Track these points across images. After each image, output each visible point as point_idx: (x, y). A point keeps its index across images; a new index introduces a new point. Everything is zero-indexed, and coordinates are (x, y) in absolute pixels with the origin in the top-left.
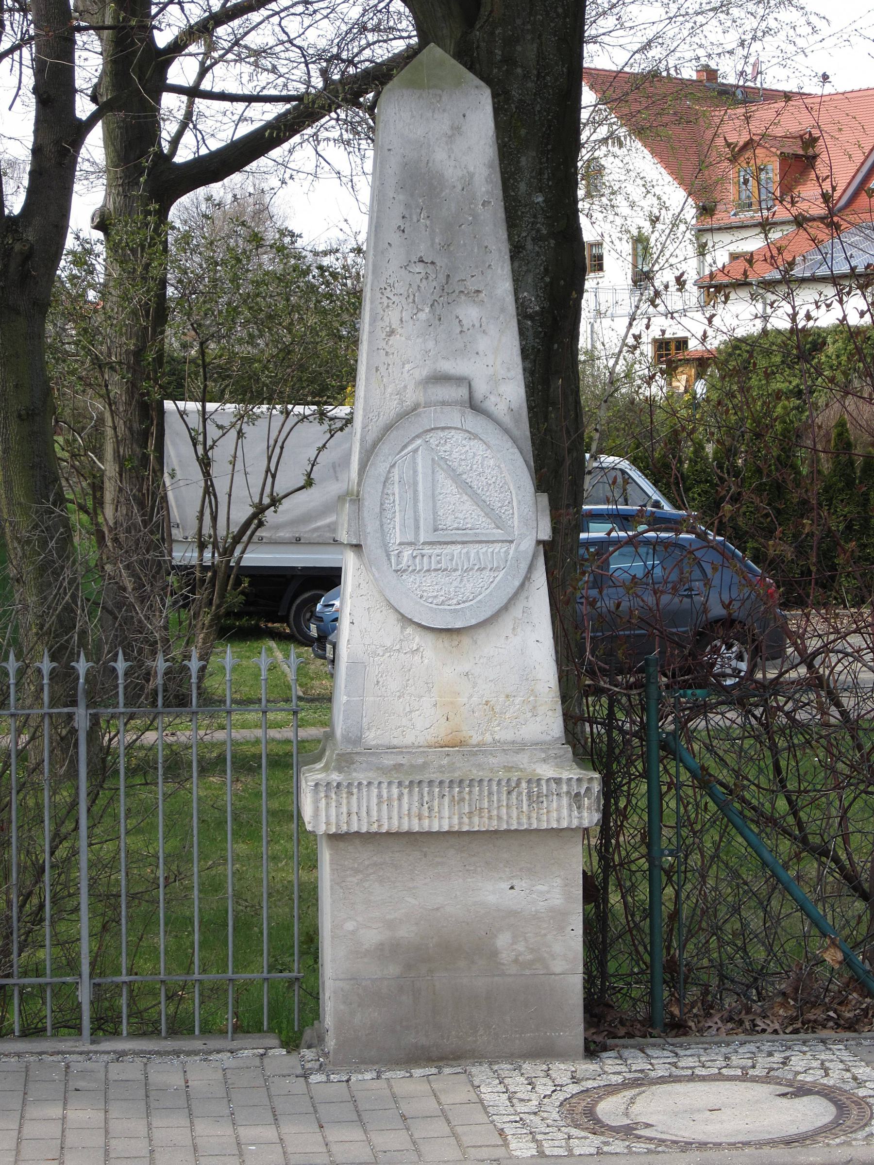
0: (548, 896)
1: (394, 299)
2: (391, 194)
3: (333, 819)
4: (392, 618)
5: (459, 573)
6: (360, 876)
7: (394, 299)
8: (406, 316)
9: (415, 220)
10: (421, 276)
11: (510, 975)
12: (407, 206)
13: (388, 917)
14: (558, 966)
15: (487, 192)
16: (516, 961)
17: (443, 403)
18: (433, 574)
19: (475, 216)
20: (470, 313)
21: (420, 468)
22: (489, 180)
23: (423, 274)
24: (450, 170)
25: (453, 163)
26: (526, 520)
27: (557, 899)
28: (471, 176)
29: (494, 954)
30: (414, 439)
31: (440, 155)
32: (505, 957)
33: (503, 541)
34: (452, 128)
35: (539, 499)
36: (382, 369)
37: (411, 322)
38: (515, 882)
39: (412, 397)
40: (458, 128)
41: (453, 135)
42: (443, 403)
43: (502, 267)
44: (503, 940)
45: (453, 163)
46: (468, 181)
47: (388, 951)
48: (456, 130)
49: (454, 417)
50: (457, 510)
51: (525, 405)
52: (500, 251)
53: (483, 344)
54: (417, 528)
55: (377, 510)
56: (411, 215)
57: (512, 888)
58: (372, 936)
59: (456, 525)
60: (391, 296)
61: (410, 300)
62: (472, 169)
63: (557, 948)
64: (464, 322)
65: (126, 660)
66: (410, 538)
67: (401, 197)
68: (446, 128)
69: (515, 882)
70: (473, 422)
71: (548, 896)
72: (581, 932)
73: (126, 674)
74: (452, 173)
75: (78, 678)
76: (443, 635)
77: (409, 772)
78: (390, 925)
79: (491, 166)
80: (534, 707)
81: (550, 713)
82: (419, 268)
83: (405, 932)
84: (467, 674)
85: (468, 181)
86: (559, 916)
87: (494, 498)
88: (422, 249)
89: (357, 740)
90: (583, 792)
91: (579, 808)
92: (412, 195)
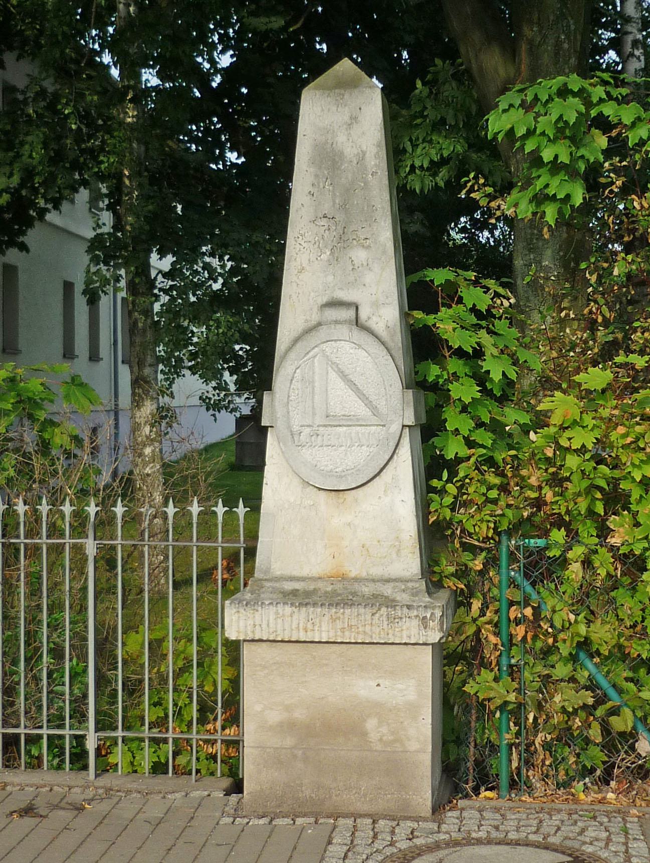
0: (405, 692)
1: (304, 245)
2: (305, 168)
3: (242, 629)
4: (296, 481)
5: (343, 448)
6: (266, 671)
7: (304, 245)
8: (313, 258)
9: (322, 186)
10: (324, 228)
11: (376, 751)
12: (316, 176)
13: (286, 703)
14: (413, 746)
15: (376, 165)
16: (381, 740)
17: (337, 322)
18: (325, 448)
19: (366, 183)
20: (360, 255)
21: (317, 370)
22: (376, 156)
23: (326, 227)
24: (348, 150)
25: (351, 144)
26: (399, 409)
27: (412, 696)
28: (364, 153)
29: (364, 734)
30: (313, 348)
31: (341, 138)
32: (373, 736)
33: (377, 425)
34: (351, 118)
35: (405, 394)
36: (294, 297)
37: (316, 262)
38: (380, 681)
39: (315, 318)
40: (356, 118)
41: (352, 123)
42: (337, 322)
43: (385, 221)
44: (371, 724)
45: (351, 144)
46: (361, 157)
47: (288, 727)
48: (354, 119)
49: (344, 331)
50: (341, 399)
51: (399, 324)
52: (383, 208)
53: (369, 278)
54: (314, 414)
55: (286, 400)
56: (319, 183)
57: (378, 685)
58: (274, 717)
59: (343, 413)
60: (302, 243)
61: (316, 246)
62: (364, 148)
63: (412, 732)
64: (355, 262)
65: (175, 507)
66: (309, 422)
67: (312, 170)
68: (347, 118)
69: (380, 681)
70: (358, 335)
71: (405, 692)
72: (430, 721)
73: (123, 516)
74: (350, 151)
75: (238, 520)
76: (333, 493)
77: (301, 597)
78: (288, 708)
79: (378, 146)
80: (399, 550)
81: (410, 555)
82: (324, 222)
83: (299, 715)
84: (349, 524)
85: (361, 157)
86: (412, 709)
87: (371, 392)
88: (327, 208)
89: (267, 571)
90: (428, 616)
91: (425, 628)
92: (320, 168)
